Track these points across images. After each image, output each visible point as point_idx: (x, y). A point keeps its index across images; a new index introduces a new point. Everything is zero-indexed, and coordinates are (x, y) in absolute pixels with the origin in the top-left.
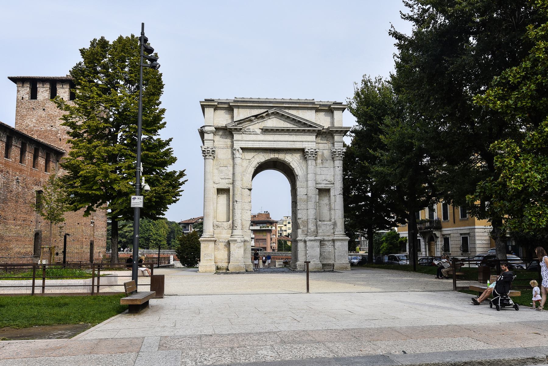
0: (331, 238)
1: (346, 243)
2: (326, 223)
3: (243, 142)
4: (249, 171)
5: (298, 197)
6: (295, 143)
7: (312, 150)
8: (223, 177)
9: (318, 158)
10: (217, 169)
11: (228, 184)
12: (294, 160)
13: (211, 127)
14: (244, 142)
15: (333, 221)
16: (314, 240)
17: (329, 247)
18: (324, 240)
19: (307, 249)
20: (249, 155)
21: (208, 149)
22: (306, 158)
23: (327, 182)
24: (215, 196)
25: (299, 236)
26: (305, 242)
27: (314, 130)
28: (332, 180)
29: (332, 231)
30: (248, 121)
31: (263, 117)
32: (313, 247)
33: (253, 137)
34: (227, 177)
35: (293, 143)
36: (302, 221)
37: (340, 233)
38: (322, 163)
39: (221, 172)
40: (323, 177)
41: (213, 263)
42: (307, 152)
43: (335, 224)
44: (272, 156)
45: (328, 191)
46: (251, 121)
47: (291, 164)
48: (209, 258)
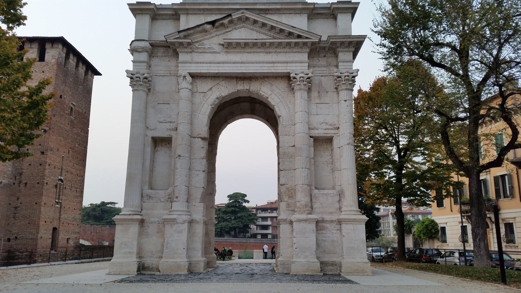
0: (335, 217)
2: (326, 191)
3: (193, 65)
6: (275, 65)
7: (302, 75)
8: (162, 120)
9: (313, 89)
11: (170, 130)
13: (143, 42)
14: (195, 65)
15: (338, 188)
16: (306, 220)
17: (331, 233)
18: (323, 221)
20: (203, 86)
21: (138, 75)
22: (293, 89)
24: (149, 149)
26: (291, 223)
27: (305, 44)
28: (336, 123)
29: (337, 205)
30: (201, 32)
31: (223, 25)
34: (168, 120)
35: (272, 65)
36: (287, 189)
37: (350, 209)
38: (319, 97)
42: (294, 78)
43: (341, 194)
44: (242, 87)
45: (329, 140)
46: (205, 31)
47: (269, 99)
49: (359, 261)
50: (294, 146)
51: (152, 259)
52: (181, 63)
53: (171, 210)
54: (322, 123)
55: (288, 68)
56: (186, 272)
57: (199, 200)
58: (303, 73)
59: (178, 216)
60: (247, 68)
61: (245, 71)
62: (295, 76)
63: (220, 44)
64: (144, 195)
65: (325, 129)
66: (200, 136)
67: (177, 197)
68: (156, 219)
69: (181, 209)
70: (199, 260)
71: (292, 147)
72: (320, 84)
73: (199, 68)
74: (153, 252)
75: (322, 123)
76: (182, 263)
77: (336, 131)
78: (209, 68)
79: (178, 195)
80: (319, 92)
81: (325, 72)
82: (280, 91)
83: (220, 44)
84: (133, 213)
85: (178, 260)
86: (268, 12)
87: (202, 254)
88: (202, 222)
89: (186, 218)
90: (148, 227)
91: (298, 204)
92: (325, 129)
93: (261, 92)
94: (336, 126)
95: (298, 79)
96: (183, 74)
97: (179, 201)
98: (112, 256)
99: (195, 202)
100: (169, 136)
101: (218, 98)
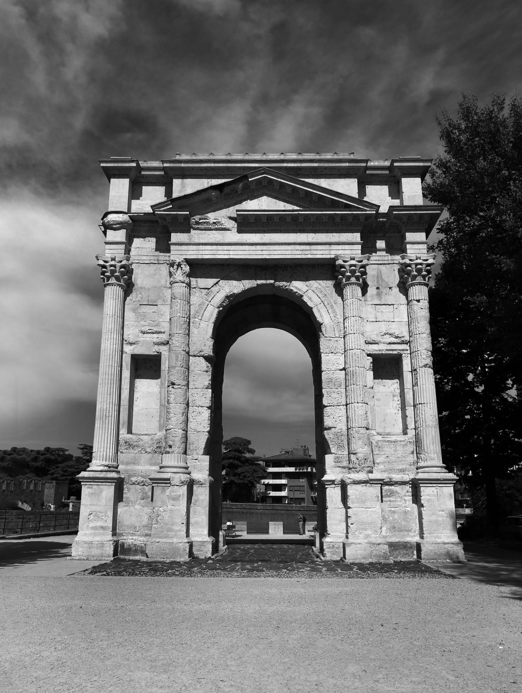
1: (450, 490)
4: (207, 314)
5: (324, 376)
8: (146, 329)
10: (134, 310)
12: (314, 293)
16: (365, 482)
19: (349, 504)
23: (393, 340)
24: (126, 374)
25: (328, 470)
32: (362, 501)
33: (220, 237)
34: (155, 329)
38: (379, 295)
39: (144, 316)
40: (383, 327)
41: (110, 537)
42: (342, 266)
47: (305, 299)
48: (99, 524)
49: (446, 541)
50: (344, 369)
51: (134, 537)
52: (175, 244)
53: (161, 465)
54: (385, 334)
55: (333, 252)
56: (186, 558)
57: (202, 451)
58: (354, 259)
59: (173, 475)
60: (271, 252)
61: (268, 257)
62: (343, 263)
63: (231, 218)
64: (121, 442)
65: (390, 343)
66: (202, 353)
67: (170, 447)
68: (140, 479)
69: (176, 464)
70: (205, 540)
71: (341, 370)
72: (379, 276)
73: (201, 252)
74: (135, 527)
75: (385, 334)
76: (181, 544)
77: (406, 347)
78: (215, 252)
79: (171, 443)
80: (378, 288)
81: (386, 258)
82: (320, 287)
83: (231, 218)
84: (106, 468)
85: (175, 540)
86: (300, 172)
87: (209, 533)
88: (208, 485)
89: (184, 477)
90: (129, 490)
91: (353, 457)
92: (390, 343)
93: (292, 288)
94: (407, 338)
95: (348, 268)
96: (178, 261)
97: (173, 452)
98: (76, 533)
99: (198, 454)
100: (156, 353)
101: (227, 297)
